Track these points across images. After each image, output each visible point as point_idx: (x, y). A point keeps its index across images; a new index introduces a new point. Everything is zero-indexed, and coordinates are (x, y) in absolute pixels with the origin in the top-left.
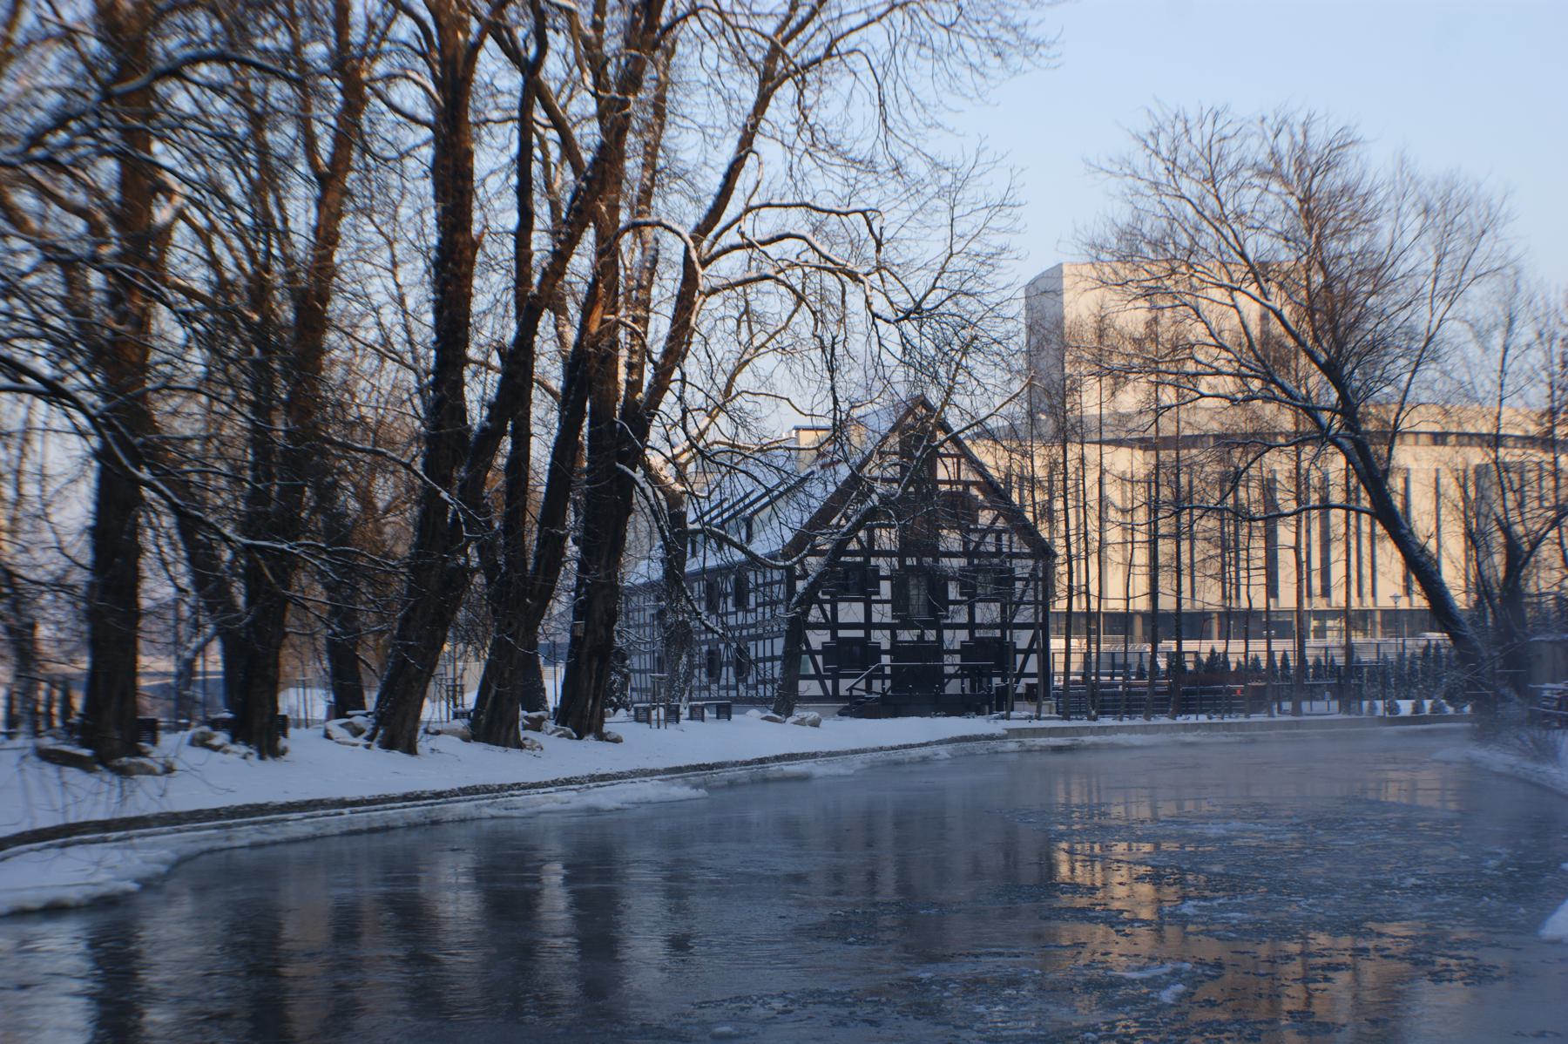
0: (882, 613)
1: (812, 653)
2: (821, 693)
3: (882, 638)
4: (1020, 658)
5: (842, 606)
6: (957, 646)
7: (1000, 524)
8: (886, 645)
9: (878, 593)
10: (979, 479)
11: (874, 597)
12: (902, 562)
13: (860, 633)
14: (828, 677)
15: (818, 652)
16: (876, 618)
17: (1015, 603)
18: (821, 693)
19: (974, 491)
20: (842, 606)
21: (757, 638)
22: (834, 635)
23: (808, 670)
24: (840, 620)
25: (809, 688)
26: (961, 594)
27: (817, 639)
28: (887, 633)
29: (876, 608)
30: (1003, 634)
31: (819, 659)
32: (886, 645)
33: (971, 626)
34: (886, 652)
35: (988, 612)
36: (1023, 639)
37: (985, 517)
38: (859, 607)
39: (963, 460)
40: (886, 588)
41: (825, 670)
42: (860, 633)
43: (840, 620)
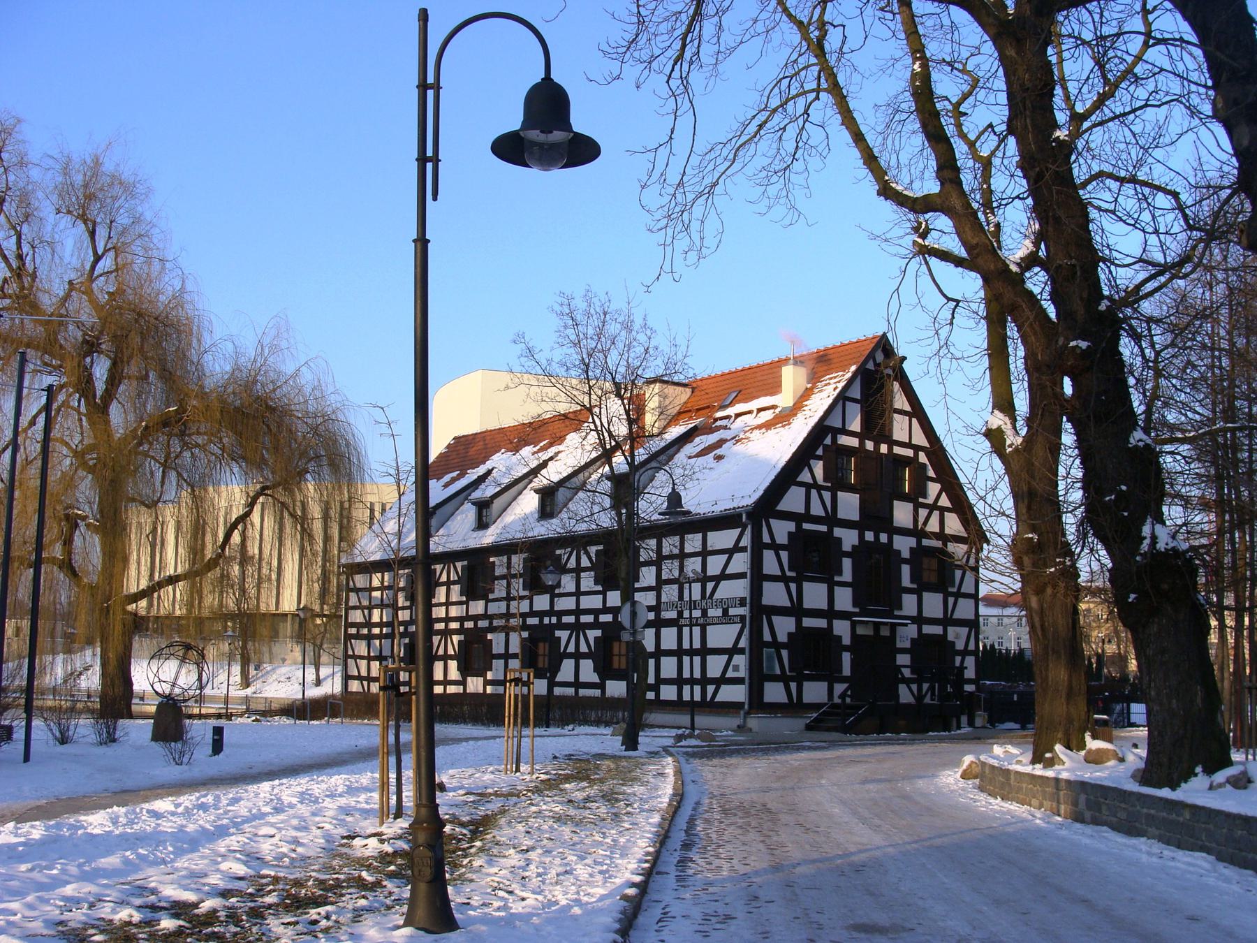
0: (844, 600)
1: (775, 644)
3: (842, 629)
4: (958, 659)
5: (807, 586)
6: (907, 645)
8: (846, 641)
9: (840, 573)
11: (837, 579)
12: (861, 536)
13: (821, 623)
14: (792, 679)
15: (784, 646)
16: (839, 606)
17: (952, 594)
19: (923, 458)
20: (806, 585)
21: (658, 624)
23: (772, 668)
24: (806, 606)
25: (774, 692)
26: (912, 582)
27: (784, 626)
28: (847, 624)
30: (945, 631)
31: (784, 653)
32: (846, 641)
33: (920, 620)
34: (846, 648)
35: (933, 604)
37: (933, 488)
38: (823, 588)
40: (847, 564)
42: (821, 623)
43: (808, 604)
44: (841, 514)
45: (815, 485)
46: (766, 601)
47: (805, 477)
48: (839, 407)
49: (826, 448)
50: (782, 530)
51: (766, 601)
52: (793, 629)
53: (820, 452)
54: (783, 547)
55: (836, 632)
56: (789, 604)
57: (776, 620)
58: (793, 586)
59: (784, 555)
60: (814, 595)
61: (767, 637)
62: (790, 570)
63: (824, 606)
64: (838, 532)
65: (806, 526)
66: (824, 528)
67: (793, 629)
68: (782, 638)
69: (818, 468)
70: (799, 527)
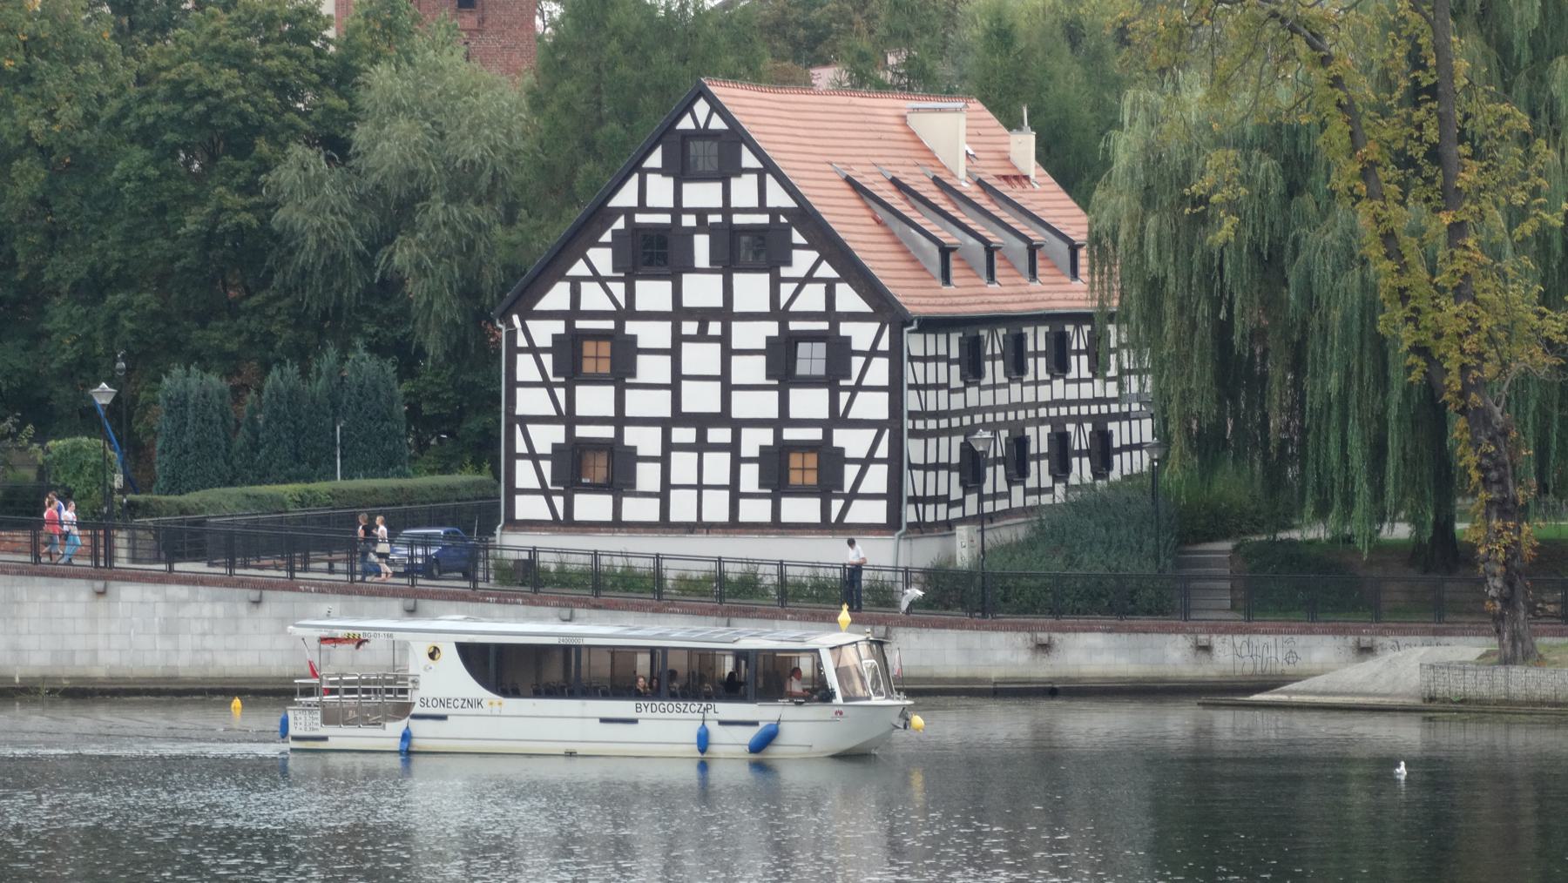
1: (533, 457)
2: (549, 517)
5: (581, 391)
7: (826, 270)
9: (633, 375)
10: (789, 203)
11: (628, 381)
14: (558, 493)
15: (544, 457)
18: (549, 517)
20: (581, 391)
22: (570, 432)
24: (578, 413)
27: (547, 437)
29: (629, 393)
31: (546, 466)
36: (853, 442)
39: (770, 179)
41: (553, 483)
42: (608, 432)
43: (581, 411)
44: (641, 305)
45: (596, 277)
46: (519, 411)
47: (579, 269)
48: (634, 180)
49: (614, 232)
50: (544, 332)
51: (519, 411)
52: (561, 439)
53: (607, 237)
54: (545, 350)
55: (628, 441)
56: (553, 412)
57: (531, 428)
58: (560, 393)
59: (547, 360)
60: (594, 400)
61: (521, 447)
62: (555, 374)
63: (611, 413)
64: (631, 327)
65: (580, 324)
66: (609, 325)
67: (561, 439)
68: (543, 447)
69: (602, 259)
70: (570, 325)
